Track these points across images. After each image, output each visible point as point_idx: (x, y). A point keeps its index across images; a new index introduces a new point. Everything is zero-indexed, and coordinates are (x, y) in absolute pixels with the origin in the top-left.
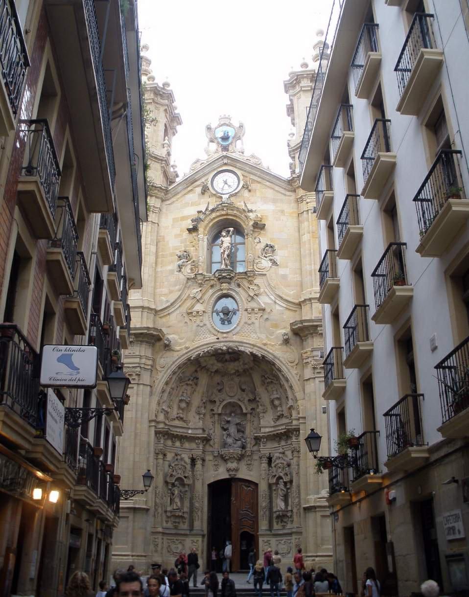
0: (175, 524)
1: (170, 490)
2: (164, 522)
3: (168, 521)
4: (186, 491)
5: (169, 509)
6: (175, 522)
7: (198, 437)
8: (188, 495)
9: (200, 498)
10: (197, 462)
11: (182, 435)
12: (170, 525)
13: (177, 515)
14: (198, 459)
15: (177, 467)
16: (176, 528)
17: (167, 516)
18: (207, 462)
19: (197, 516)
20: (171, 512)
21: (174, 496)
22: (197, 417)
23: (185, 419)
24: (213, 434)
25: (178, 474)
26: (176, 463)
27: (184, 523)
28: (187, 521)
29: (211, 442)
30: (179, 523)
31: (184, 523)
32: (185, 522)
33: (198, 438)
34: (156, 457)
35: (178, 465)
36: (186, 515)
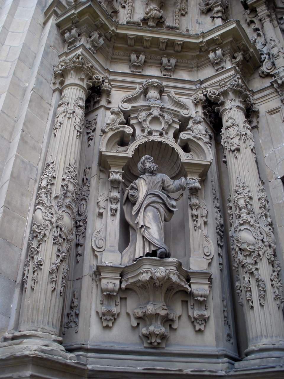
0: (144, 331)
1: (114, 184)
2: (94, 320)
3: (115, 317)
4: (194, 191)
5: (112, 258)
6: (143, 319)
7: (212, 39)
8: (207, 206)
9: (257, 210)
10: (223, 104)
11: (155, 42)
12: (121, 334)
13: (145, 277)
14: (225, 94)
15: (143, 114)
16: (155, 345)
17: (102, 291)
18: (264, 119)
19: (253, 285)
20: (122, 273)
21: (136, 208)
22: (208, 19)
23: (169, 22)
24: (265, 50)
25: (150, 133)
26: (141, 103)
27: (199, 323)
28: (214, 311)
29: (265, 67)
30: (168, 321)
31: (199, 323)
32: (205, 320)
33: (214, 44)
34: (57, 86)
35: (149, 108)
36: (198, 288)
